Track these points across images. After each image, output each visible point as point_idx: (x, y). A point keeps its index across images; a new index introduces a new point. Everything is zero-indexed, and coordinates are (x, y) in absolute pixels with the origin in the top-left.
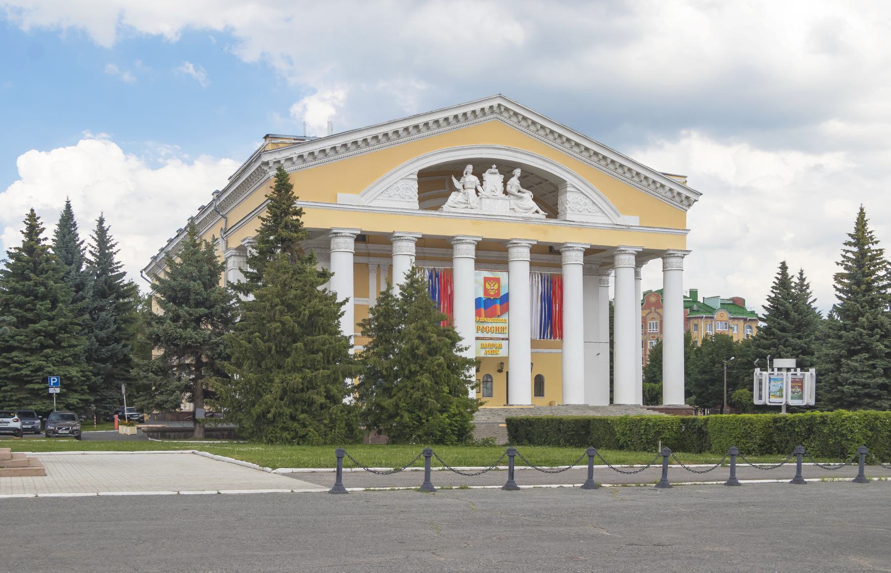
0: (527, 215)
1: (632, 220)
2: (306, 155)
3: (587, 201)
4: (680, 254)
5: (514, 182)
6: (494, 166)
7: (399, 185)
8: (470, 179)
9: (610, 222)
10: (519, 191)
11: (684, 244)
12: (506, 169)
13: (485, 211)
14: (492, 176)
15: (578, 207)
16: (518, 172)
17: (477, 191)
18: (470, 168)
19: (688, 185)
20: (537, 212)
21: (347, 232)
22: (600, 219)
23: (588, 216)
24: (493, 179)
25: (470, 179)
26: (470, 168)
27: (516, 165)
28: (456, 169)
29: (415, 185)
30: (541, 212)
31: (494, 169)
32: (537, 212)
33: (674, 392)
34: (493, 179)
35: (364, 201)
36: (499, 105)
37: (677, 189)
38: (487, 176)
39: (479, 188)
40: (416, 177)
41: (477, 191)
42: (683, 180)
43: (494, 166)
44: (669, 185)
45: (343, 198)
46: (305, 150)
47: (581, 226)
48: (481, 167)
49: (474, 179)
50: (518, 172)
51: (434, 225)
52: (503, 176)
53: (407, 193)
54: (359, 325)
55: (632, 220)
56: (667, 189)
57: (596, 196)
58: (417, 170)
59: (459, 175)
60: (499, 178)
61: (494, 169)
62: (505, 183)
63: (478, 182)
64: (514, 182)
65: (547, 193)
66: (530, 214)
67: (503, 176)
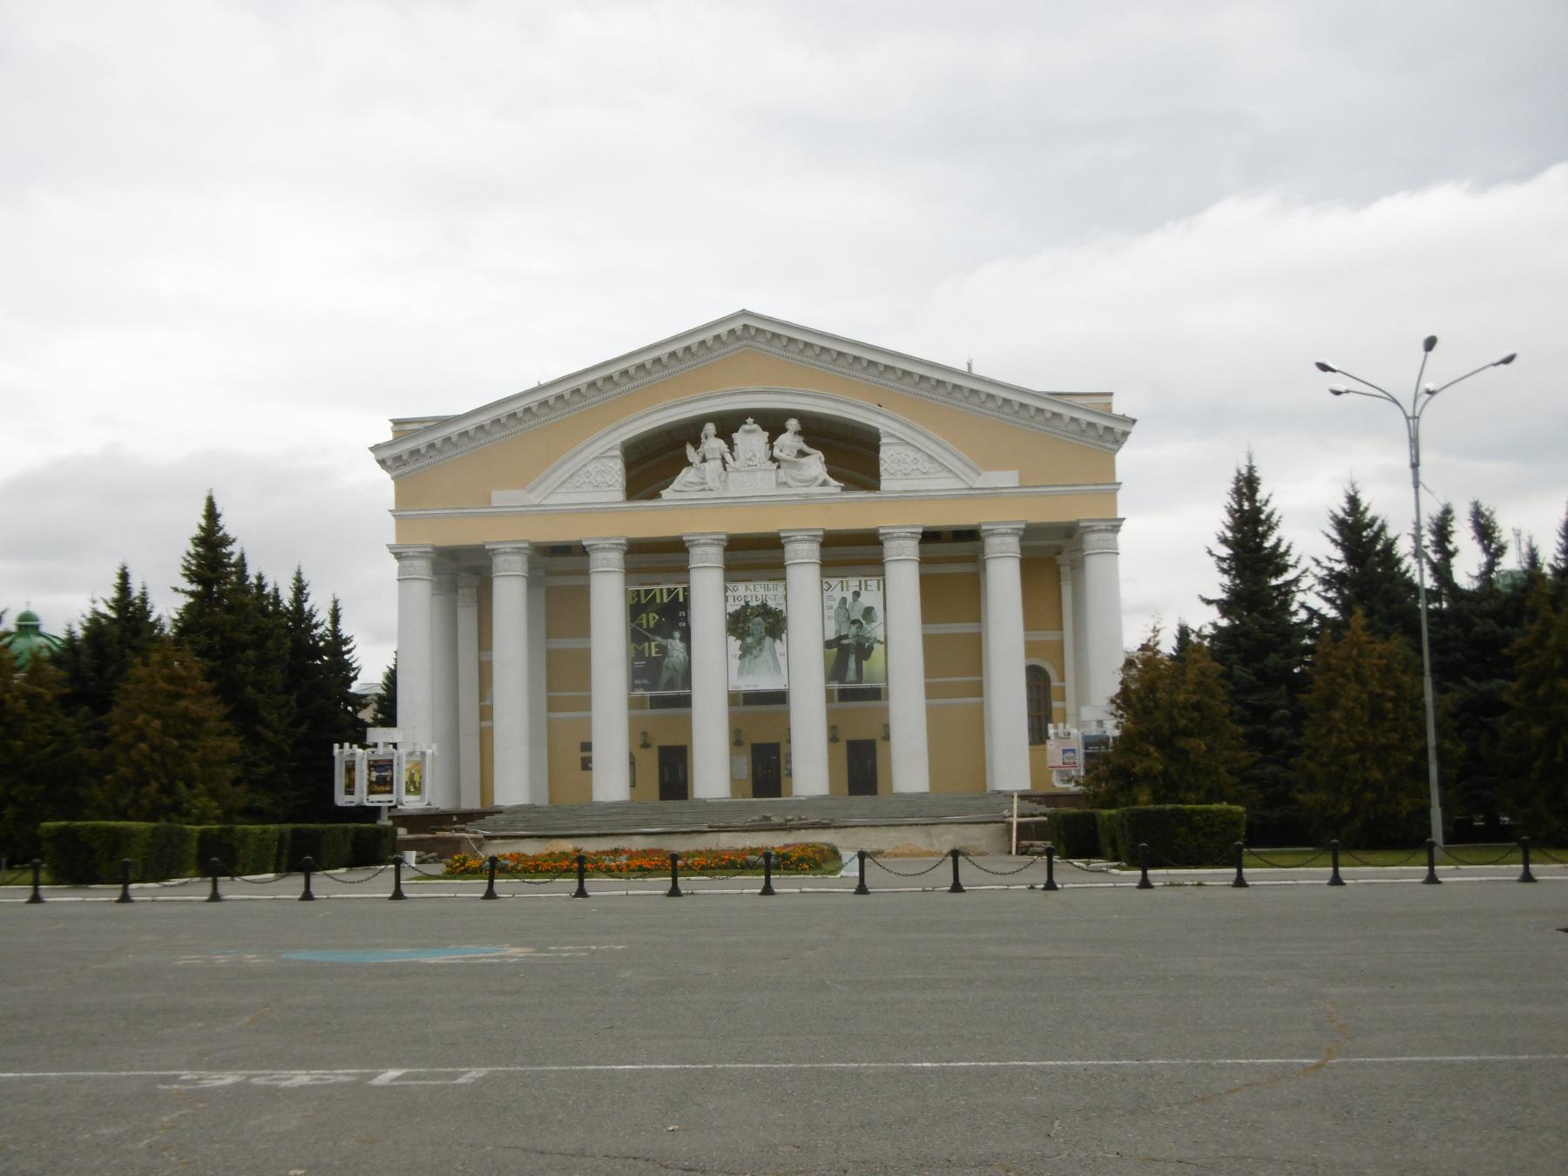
0: (806, 490)
1: (1006, 479)
2: (438, 445)
3: (919, 456)
4: (1103, 525)
5: (789, 441)
6: (750, 420)
7: (590, 468)
8: (713, 444)
9: (960, 485)
10: (802, 454)
11: (1114, 509)
12: (772, 423)
13: (734, 490)
14: (751, 436)
15: (903, 466)
16: (793, 424)
18: (710, 428)
19: (1117, 409)
20: (824, 484)
21: (605, 544)
23: (922, 478)
24: (751, 440)
25: (713, 444)
28: (689, 432)
30: (833, 482)
32: (824, 484)
34: (751, 440)
35: (533, 498)
36: (746, 326)
37: (1085, 417)
38: (738, 437)
39: (728, 457)
40: (618, 453)
42: (1105, 400)
43: (750, 420)
44: (1068, 413)
45: (503, 498)
46: (437, 436)
47: (905, 498)
48: (728, 425)
50: (793, 424)
52: (767, 434)
55: (1006, 479)
56: (1067, 420)
57: (934, 447)
58: (618, 442)
59: (697, 443)
62: (772, 440)
64: (789, 441)
65: (851, 453)
66: (815, 489)
67: (767, 434)
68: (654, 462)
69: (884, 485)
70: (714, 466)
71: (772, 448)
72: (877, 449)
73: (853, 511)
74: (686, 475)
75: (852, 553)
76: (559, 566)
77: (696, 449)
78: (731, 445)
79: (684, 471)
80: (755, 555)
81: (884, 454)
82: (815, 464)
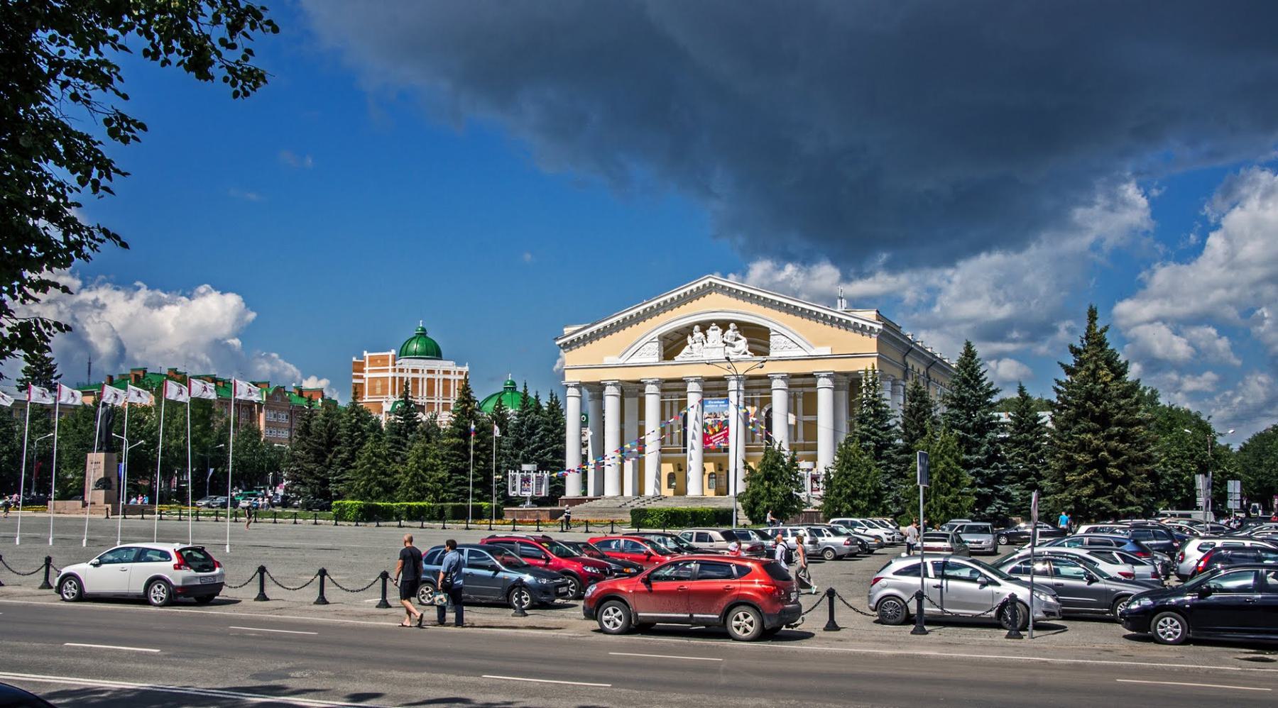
12: (724, 325)
18: (697, 328)
22: (799, 353)
24: (714, 334)
25: (698, 335)
26: (697, 328)
27: (732, 321)
28: (689, 330)
29: (656, 345)
31: (714, 326)
34: (714, 334)
35: (621, 361)
38: (709, 332)
48: (704, 326)
49: (701, 335)
50: (732, 325)
53: (652, 353)
59: (692, 335)
60: (720, 331)
61: (714, 326)
65: (758, 337)
69: (774, 354)
72: (769, 337)
74: (687, 349)
75: (757, 388)
80: (714, 388)
81: (772, 339)
82: (742, 344)
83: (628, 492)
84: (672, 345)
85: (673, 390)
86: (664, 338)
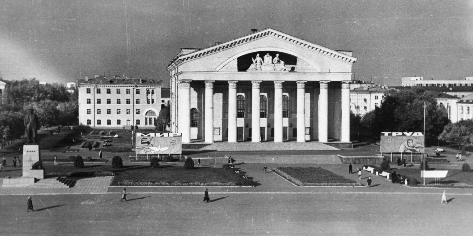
5: (276, 59)
8: (258, 59)
12: (273, 54)
16: (278, 55)
17: (261, 63)
18: (258, 55)
24: (268, 58)
25: (258, 59)
26: (258, 55)
28: (253, 55)
31: (268, 55)
33: (345, 137)
34: (268, 58)
38: (265, 57)
39: (262, 62)
41: (261, 63)
48: (262, 54)
49: (261, 58)
50: (278, 55)
51: (244, 76)
52: (271, 57)
54: (124, 128)
59: (254, 59)
60: (271, 57)
61: (268, 55)
62: (273, 59)
63: (261, 60)
68: (244, 63)
70: (259, 63)
71: (273, 60)
73: (291, 77)
74: (252, 66)
76: (221, 87)
77: (254, 59)
78: (263, 59)
79: (252, 65)
80: (267, 87)
83: (323, 135)
84: (244, 63)
85: (245, 87)
86: (240, 59)
